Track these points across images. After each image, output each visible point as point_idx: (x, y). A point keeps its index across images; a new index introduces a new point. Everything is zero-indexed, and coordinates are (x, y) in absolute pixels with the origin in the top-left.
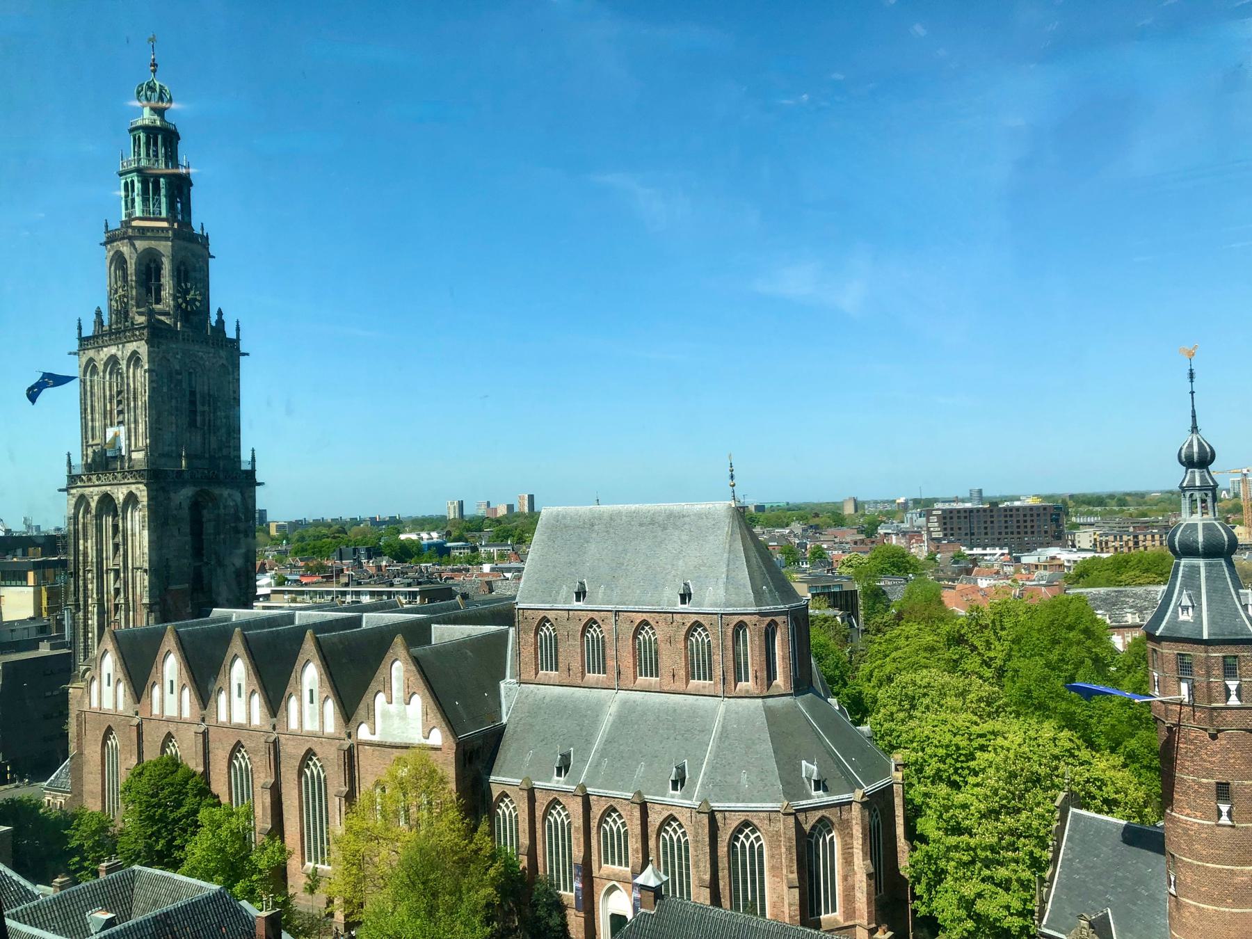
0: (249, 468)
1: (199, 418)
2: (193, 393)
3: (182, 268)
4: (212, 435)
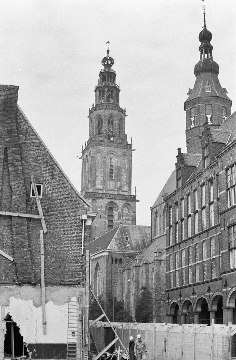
0: (134, 195)
1: (114, 175)
3: (111, 120)
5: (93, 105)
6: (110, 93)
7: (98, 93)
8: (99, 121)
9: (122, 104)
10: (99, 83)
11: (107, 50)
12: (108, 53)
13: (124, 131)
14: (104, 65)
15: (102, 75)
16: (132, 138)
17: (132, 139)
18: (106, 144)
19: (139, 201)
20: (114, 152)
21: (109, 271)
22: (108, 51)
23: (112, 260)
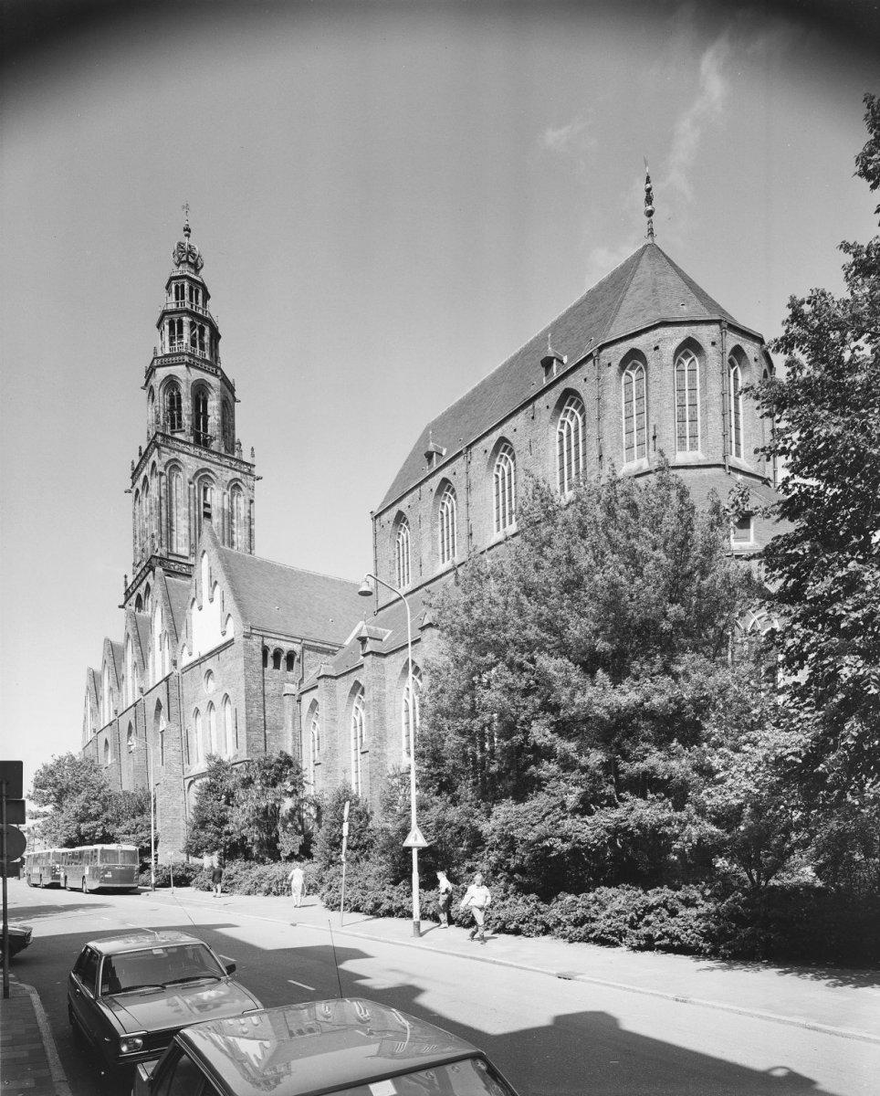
3: (201, 397)
5: (155, 353)
6: (198, 332)
7: (167, 327)
8: (172, 396)
16: (253, 449)
21: (254, 687)
23: (265, 651)
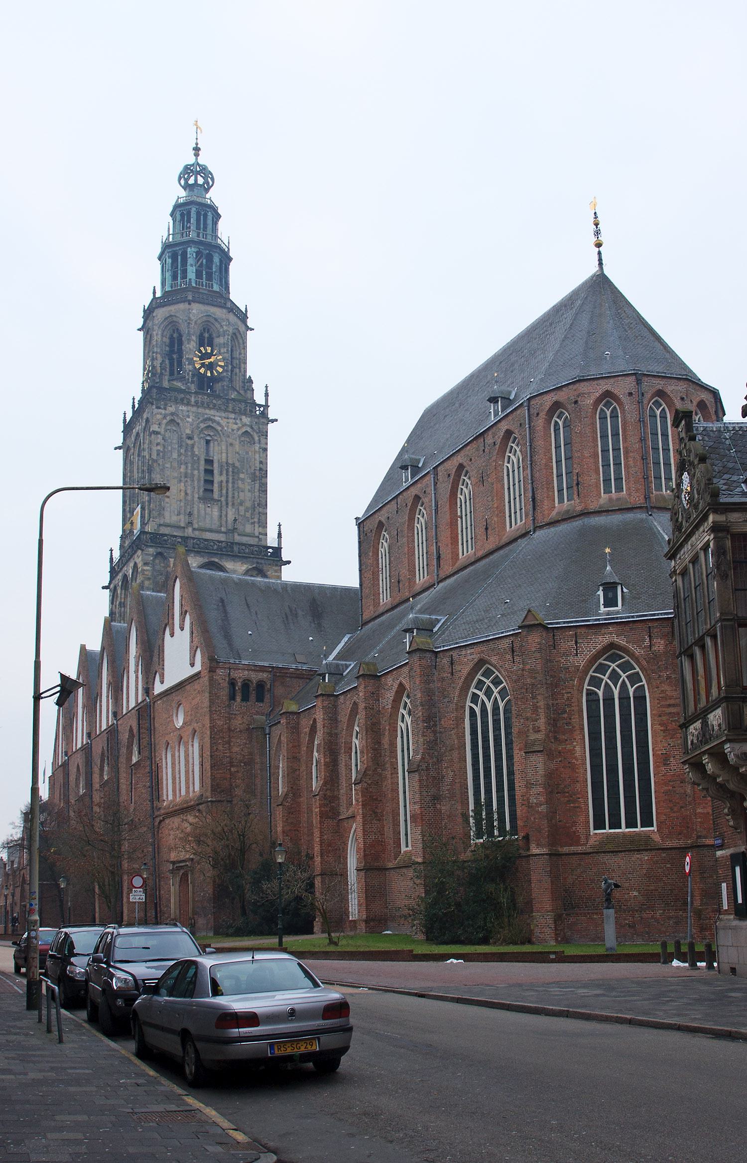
1: (216, 487)
2: (209, 462)
3: (206, 335)
4: (230, 507)
5: (154, 293)
9: (238, 295)
10: (171, 232)
11: (195, 146)
12: (197, 155)
13: (242, 370)
14: (184, 188)
15: (181, 212)
16: (267, 387)
17: (267, 390)
18: (193, 399)
19: (289, 562)
20: (219, 423)
22: (197, 150)
